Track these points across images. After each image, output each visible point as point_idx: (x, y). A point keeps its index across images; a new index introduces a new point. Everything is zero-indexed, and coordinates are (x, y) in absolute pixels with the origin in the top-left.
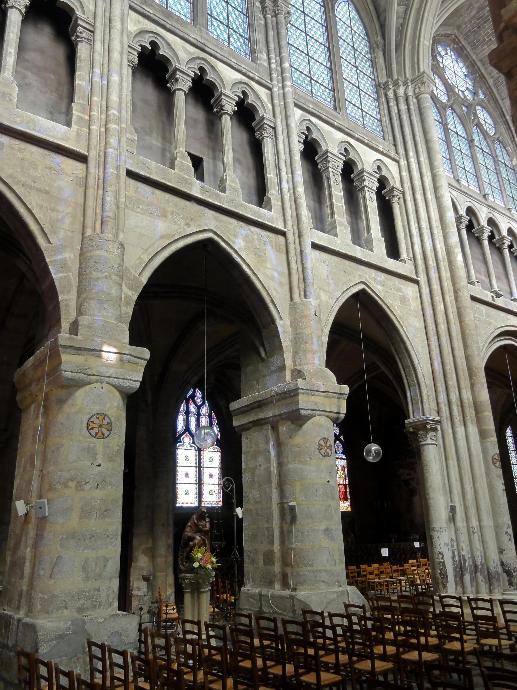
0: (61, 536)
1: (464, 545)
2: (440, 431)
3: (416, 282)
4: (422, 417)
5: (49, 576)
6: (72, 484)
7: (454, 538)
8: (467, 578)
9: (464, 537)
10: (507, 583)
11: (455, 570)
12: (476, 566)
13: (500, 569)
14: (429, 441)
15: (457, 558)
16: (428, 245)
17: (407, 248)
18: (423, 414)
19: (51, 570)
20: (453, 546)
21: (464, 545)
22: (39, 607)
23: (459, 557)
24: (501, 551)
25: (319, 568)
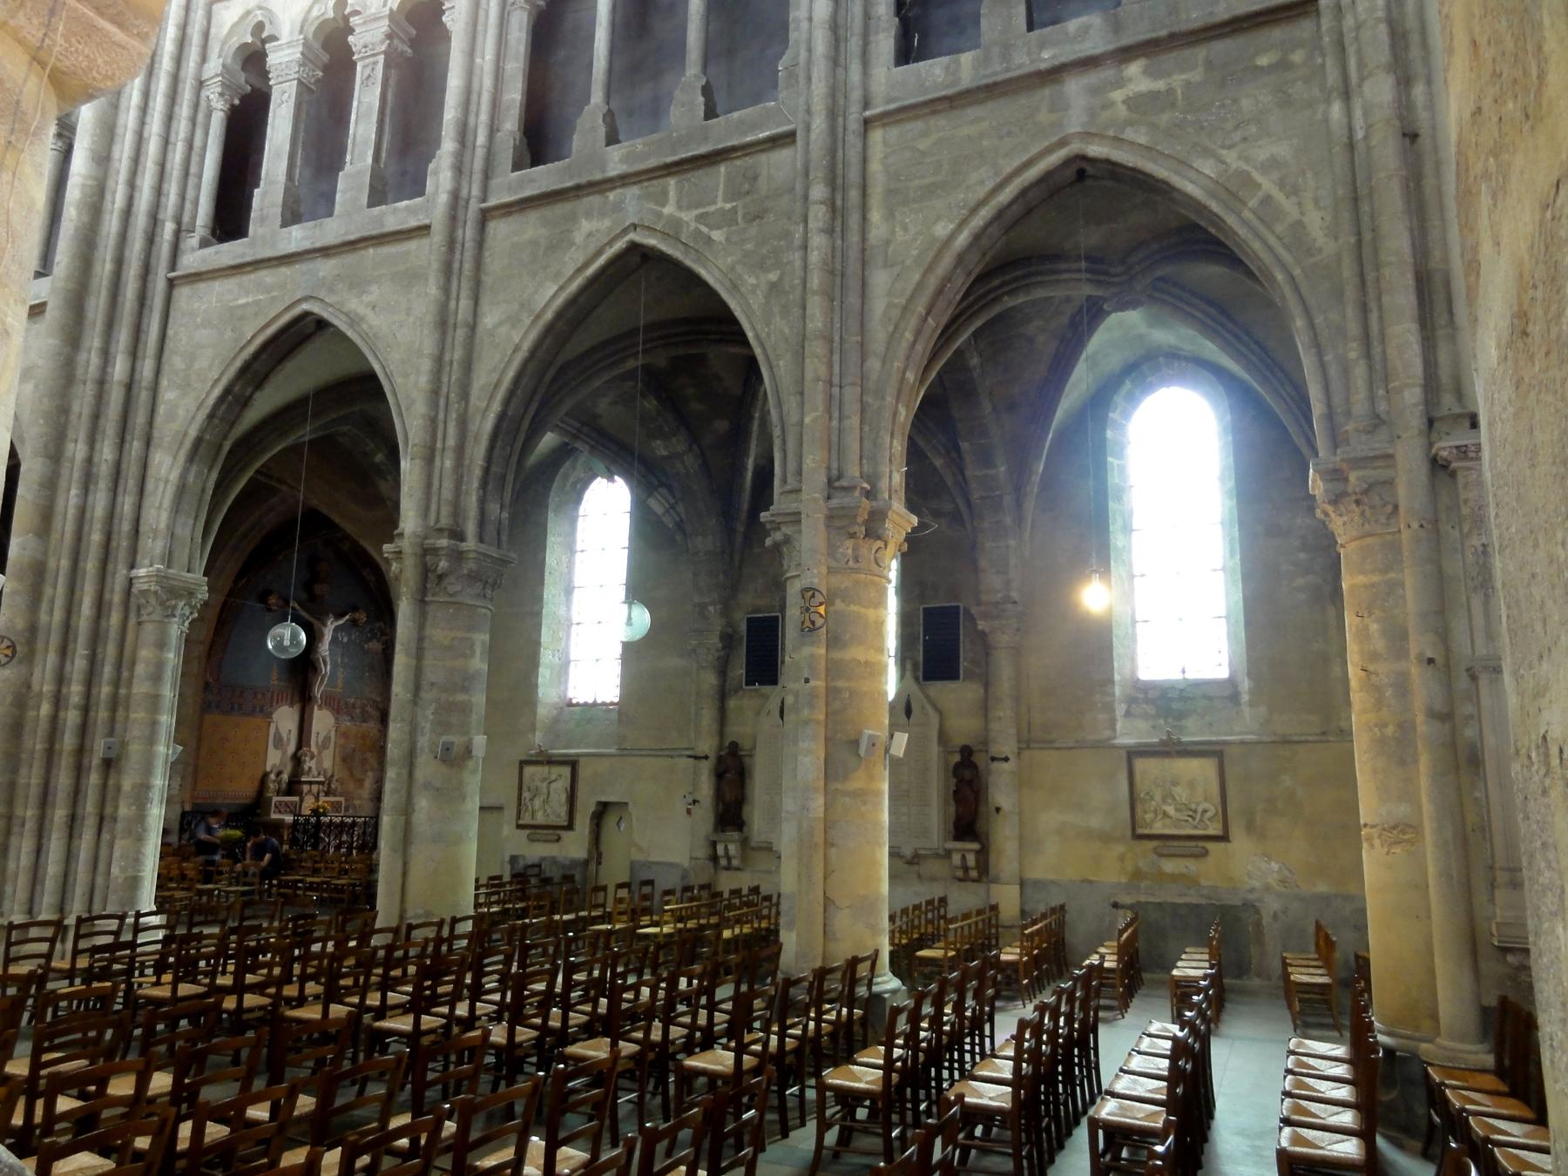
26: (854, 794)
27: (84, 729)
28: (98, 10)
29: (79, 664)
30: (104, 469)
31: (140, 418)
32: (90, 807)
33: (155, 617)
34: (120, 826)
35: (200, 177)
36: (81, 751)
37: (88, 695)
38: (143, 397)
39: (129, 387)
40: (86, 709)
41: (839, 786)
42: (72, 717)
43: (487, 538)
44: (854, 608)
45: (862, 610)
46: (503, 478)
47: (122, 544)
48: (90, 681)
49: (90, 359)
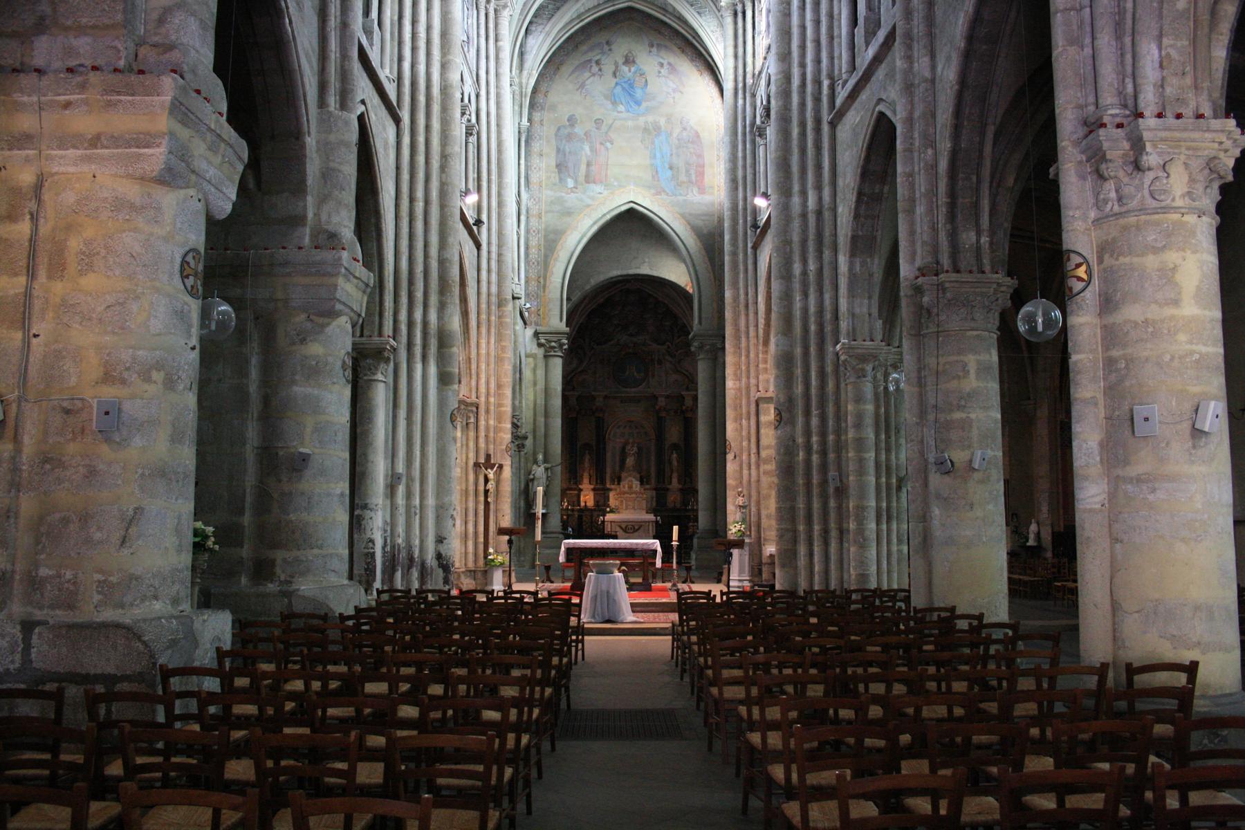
0: (140, 471)
1: (401, 530)
2: (392, 364)
3: (397, 120)
4: (376, 339)
5: (119, 542)
6: (157, 376)
7: (389, 520)
8: (399, 575)
9: (401, 520)
10: (441, 581)
11: (384, 564)
12: (411, 559)
13: (435, 563)
14: (380, 377)
15: (388, 549)
16: (422, 68)
17: (391, 60)
18: (380, 335)
19: (123, 533)
20: (385, 531)
21: (401, 530)
22: (97, 598)
23: (393, 547)
24: (440, 540)
25: (331, 551)
26: (1139, 480)
27: (824, 467)
28: (138, 147)
29: (815, 421)
30: (812, 277)
31: (827, 232)
32: (833, 525)
33: (852, 380)
34: (851, 536)
35: (840, 37)
36: (824, 483)
37: (823, 443)
38: (827, 215)
39: (819, 213)
40: (824, 453)
41: (1119, 472)
42: (815, 458)
43: (962, 266)
44: (1122, 260)
45: (1135, 260)
46: (976, 205)
47: (828, 328)
48: (823, 434)
49: (796, 200)
